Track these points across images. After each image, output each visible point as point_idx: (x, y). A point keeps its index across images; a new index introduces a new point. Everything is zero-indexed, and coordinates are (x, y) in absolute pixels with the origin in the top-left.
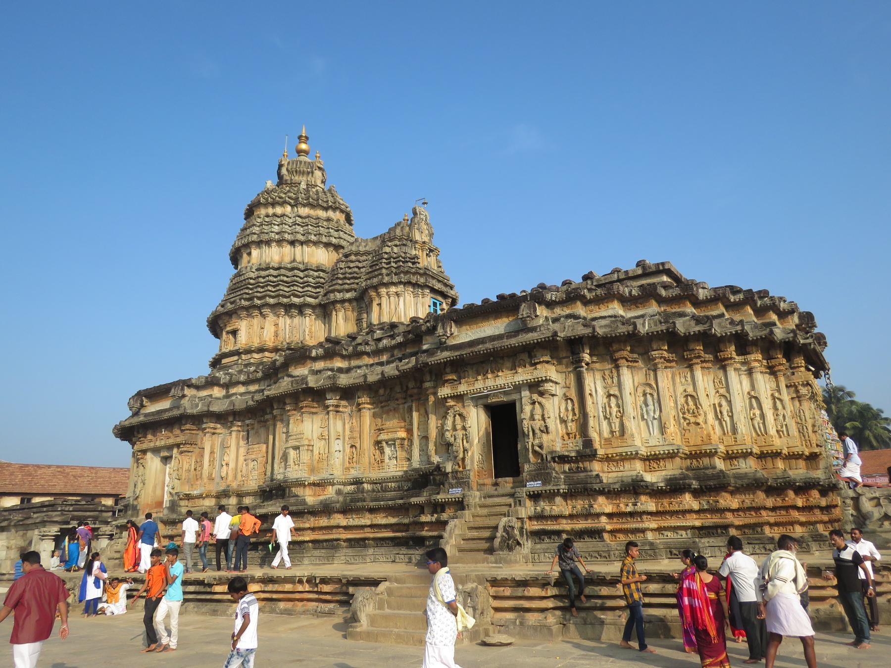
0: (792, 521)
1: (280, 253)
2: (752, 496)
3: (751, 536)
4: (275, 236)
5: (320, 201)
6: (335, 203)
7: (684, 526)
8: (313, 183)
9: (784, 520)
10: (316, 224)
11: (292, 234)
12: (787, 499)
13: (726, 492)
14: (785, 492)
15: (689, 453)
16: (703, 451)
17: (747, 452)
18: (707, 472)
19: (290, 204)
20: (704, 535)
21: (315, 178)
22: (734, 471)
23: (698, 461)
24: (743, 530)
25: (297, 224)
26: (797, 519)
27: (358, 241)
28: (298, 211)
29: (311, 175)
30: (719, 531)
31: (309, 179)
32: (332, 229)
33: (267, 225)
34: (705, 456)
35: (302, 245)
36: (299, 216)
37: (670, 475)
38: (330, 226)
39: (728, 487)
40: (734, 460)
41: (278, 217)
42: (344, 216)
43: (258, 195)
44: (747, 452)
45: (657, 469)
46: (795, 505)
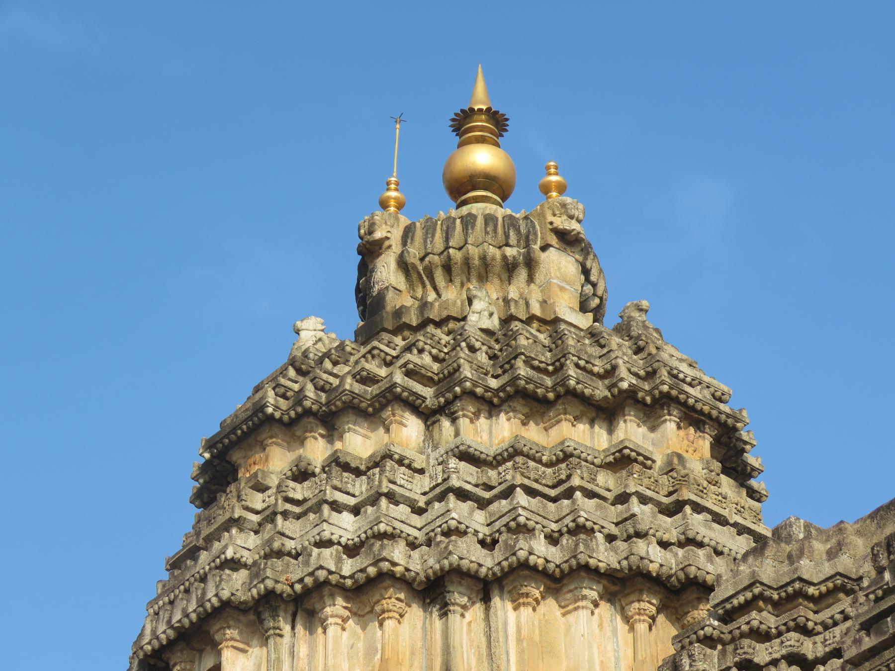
1: (370, 651)
4: (339, 561)
5: (572, 372)
6: (651, 375)
8: (536, 310)
10: (553, 487)
11: (429, 543)
19: (414, 406)
21: (546, 288)
25: (451, 490)
27: (789, 539)
28: (457, 434)
29: (523, 274)
31: (513, 293)
32: (644, 500)
33: (298, 517)
35: (486, 599)
36: (467, 456)
38: (632, 489)
41: (358, 473)
42: (705, 444)
43: (257, 389)
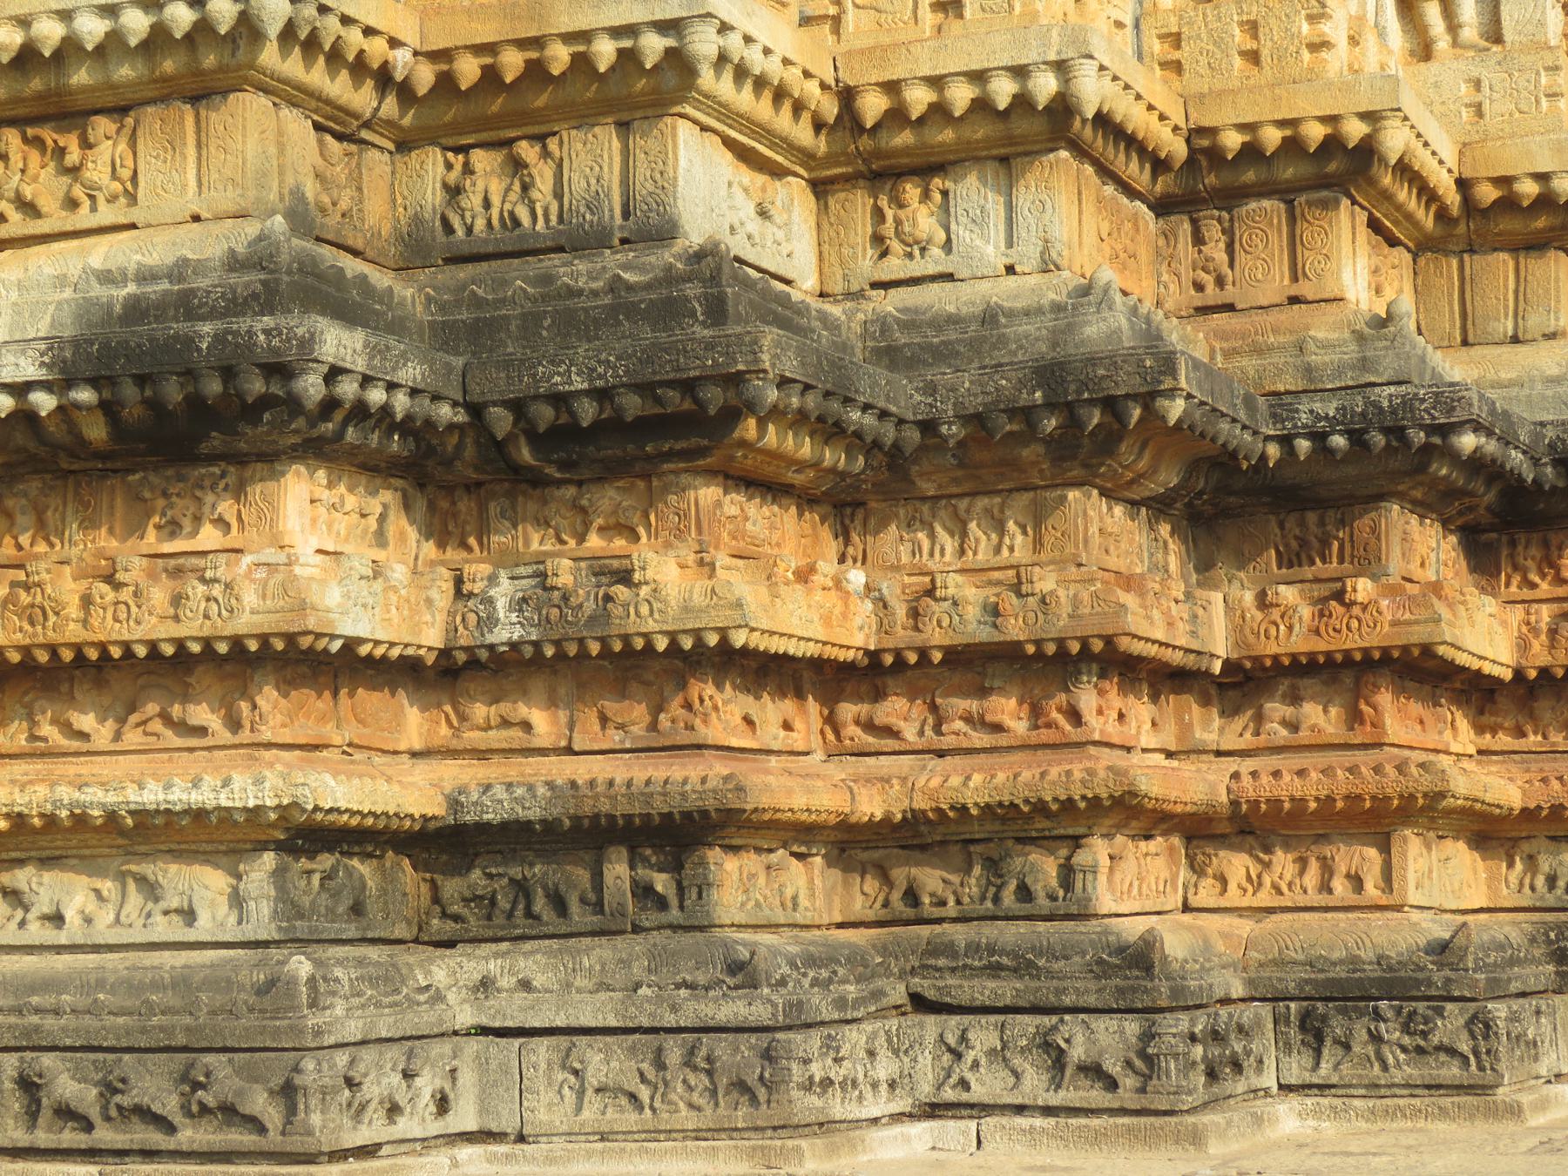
0: (1381, 801)
2: (1018, 544)
3: (960, 934)
7: (199, 815)
9: (1312, 788)
12: (1363, 588)
13: (711, 473)
14: (1363, 524)
15: (425, 77)
16: (560, 56)
17: (1022, 101)
18: (576, 272)
20: (474, 925)
22: (890, 303)
23: (518, 165)
24: (900, 874)
26: (1426, 783)
30: (618, 871)
34: (583, 117)
37: (146, 276)
39: (732, 415)
40: (911, 191)
44: (1022, 101)
45: (56, 220)
46: (1427, 650)
